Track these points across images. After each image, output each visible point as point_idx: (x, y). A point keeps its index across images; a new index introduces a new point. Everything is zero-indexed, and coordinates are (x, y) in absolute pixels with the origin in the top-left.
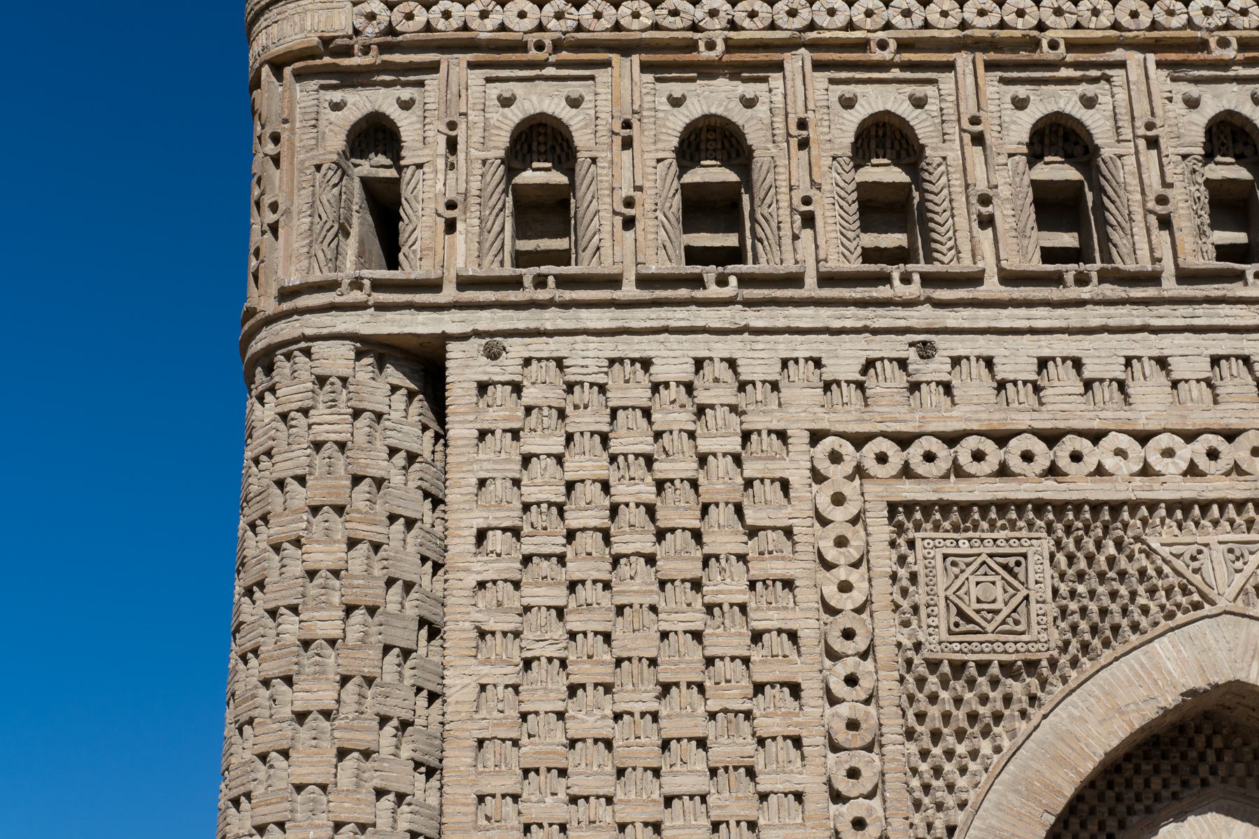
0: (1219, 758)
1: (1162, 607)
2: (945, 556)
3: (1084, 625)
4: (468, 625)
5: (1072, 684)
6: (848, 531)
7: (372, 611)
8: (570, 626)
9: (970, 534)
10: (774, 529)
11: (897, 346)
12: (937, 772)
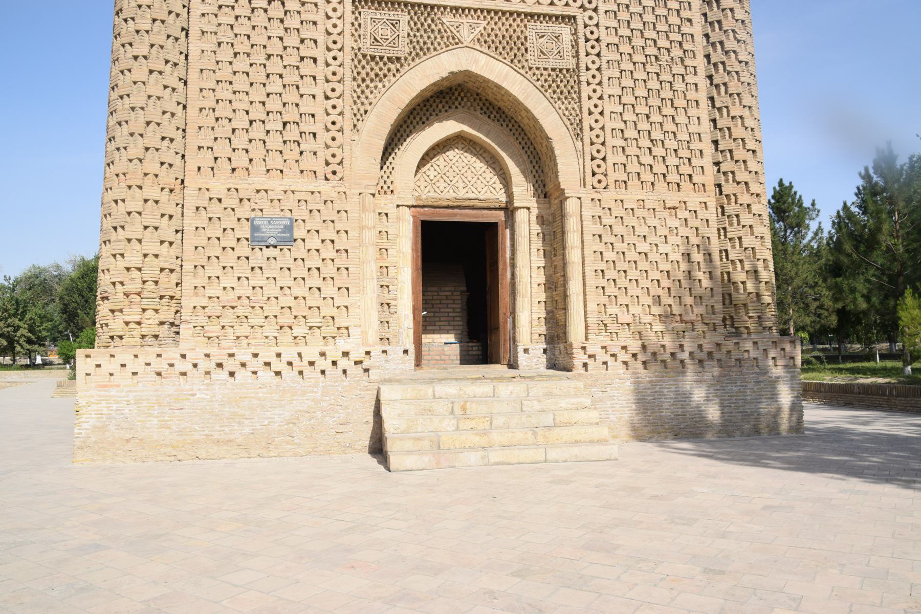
0: (462, 99)
1: (445, 43)
2: (371, 19)
3: (418, 47)
4: (198, 29)
5: (411, 66)
7: (163, 22)
8: (235, 32)
9: (381, 11)
10: (311, 3)
12: (363, 92)
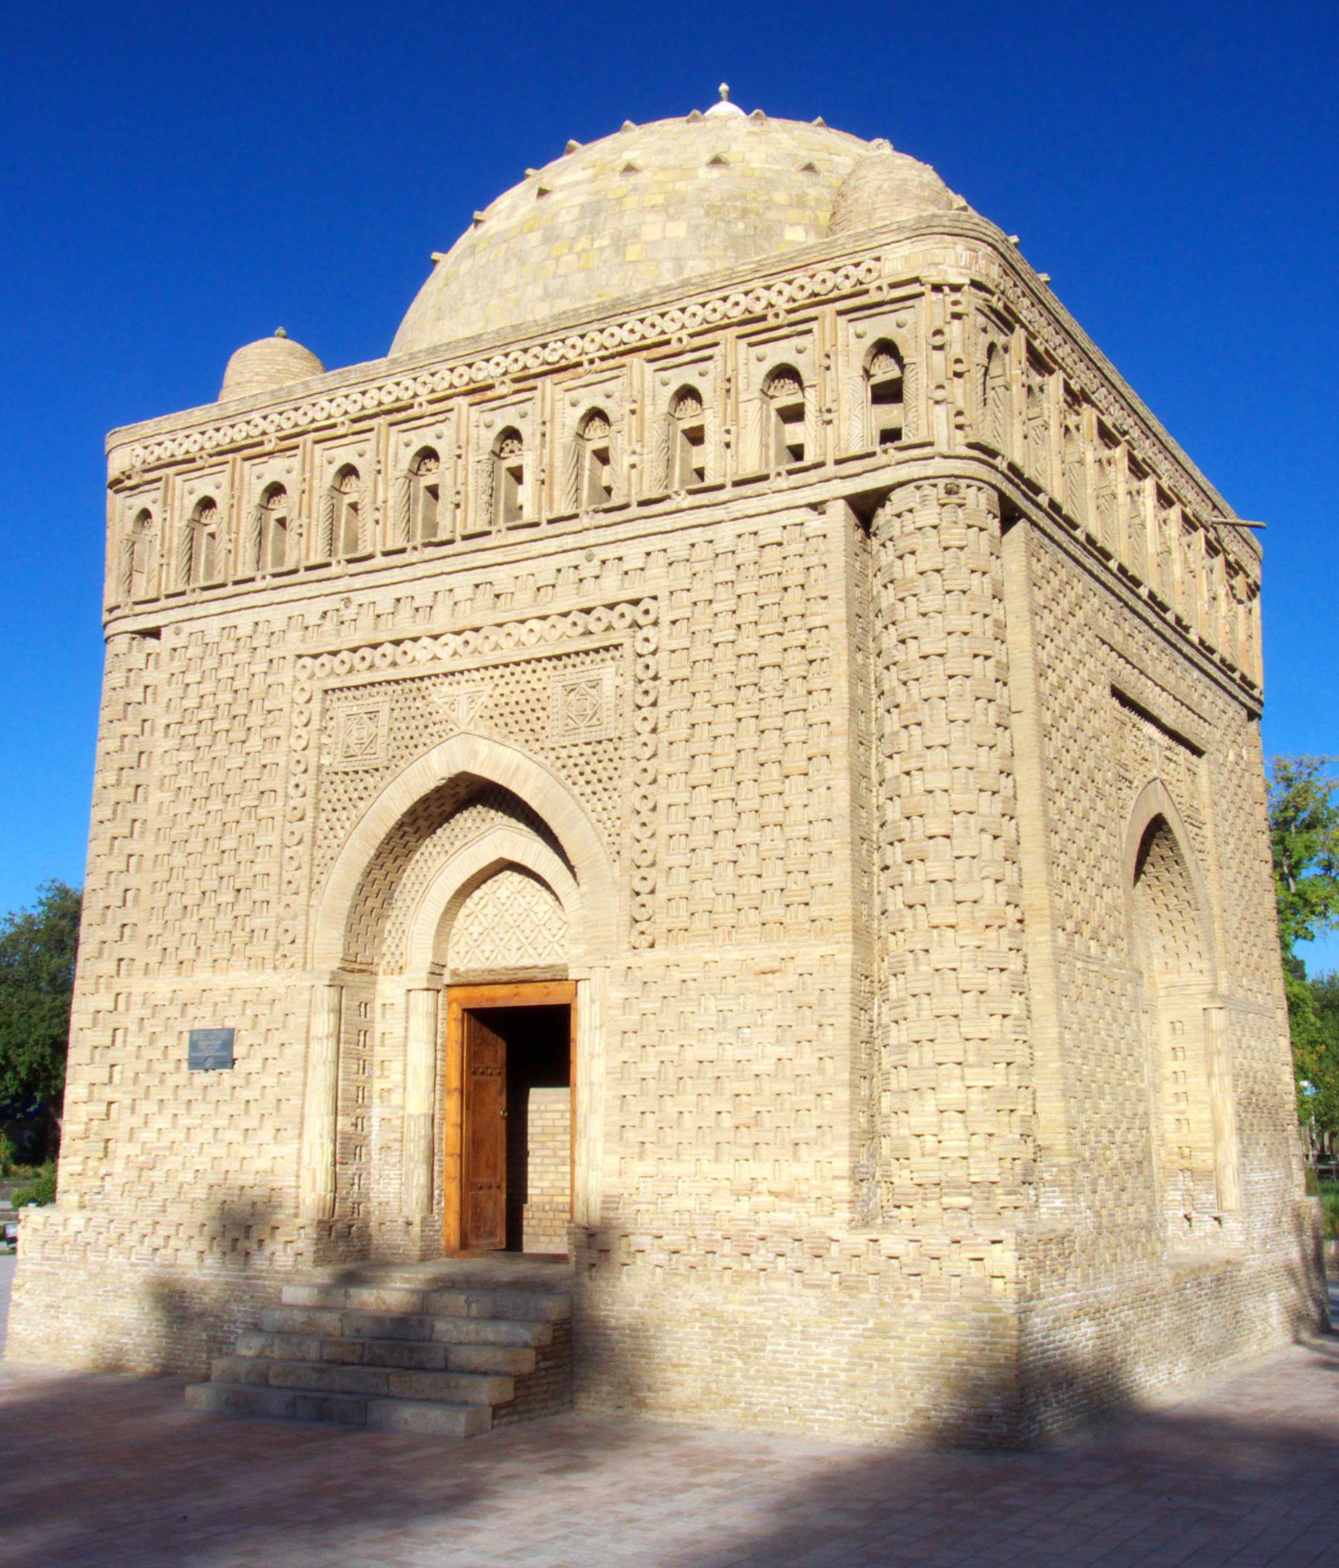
6: (303, 708)
11: (335, 602)
